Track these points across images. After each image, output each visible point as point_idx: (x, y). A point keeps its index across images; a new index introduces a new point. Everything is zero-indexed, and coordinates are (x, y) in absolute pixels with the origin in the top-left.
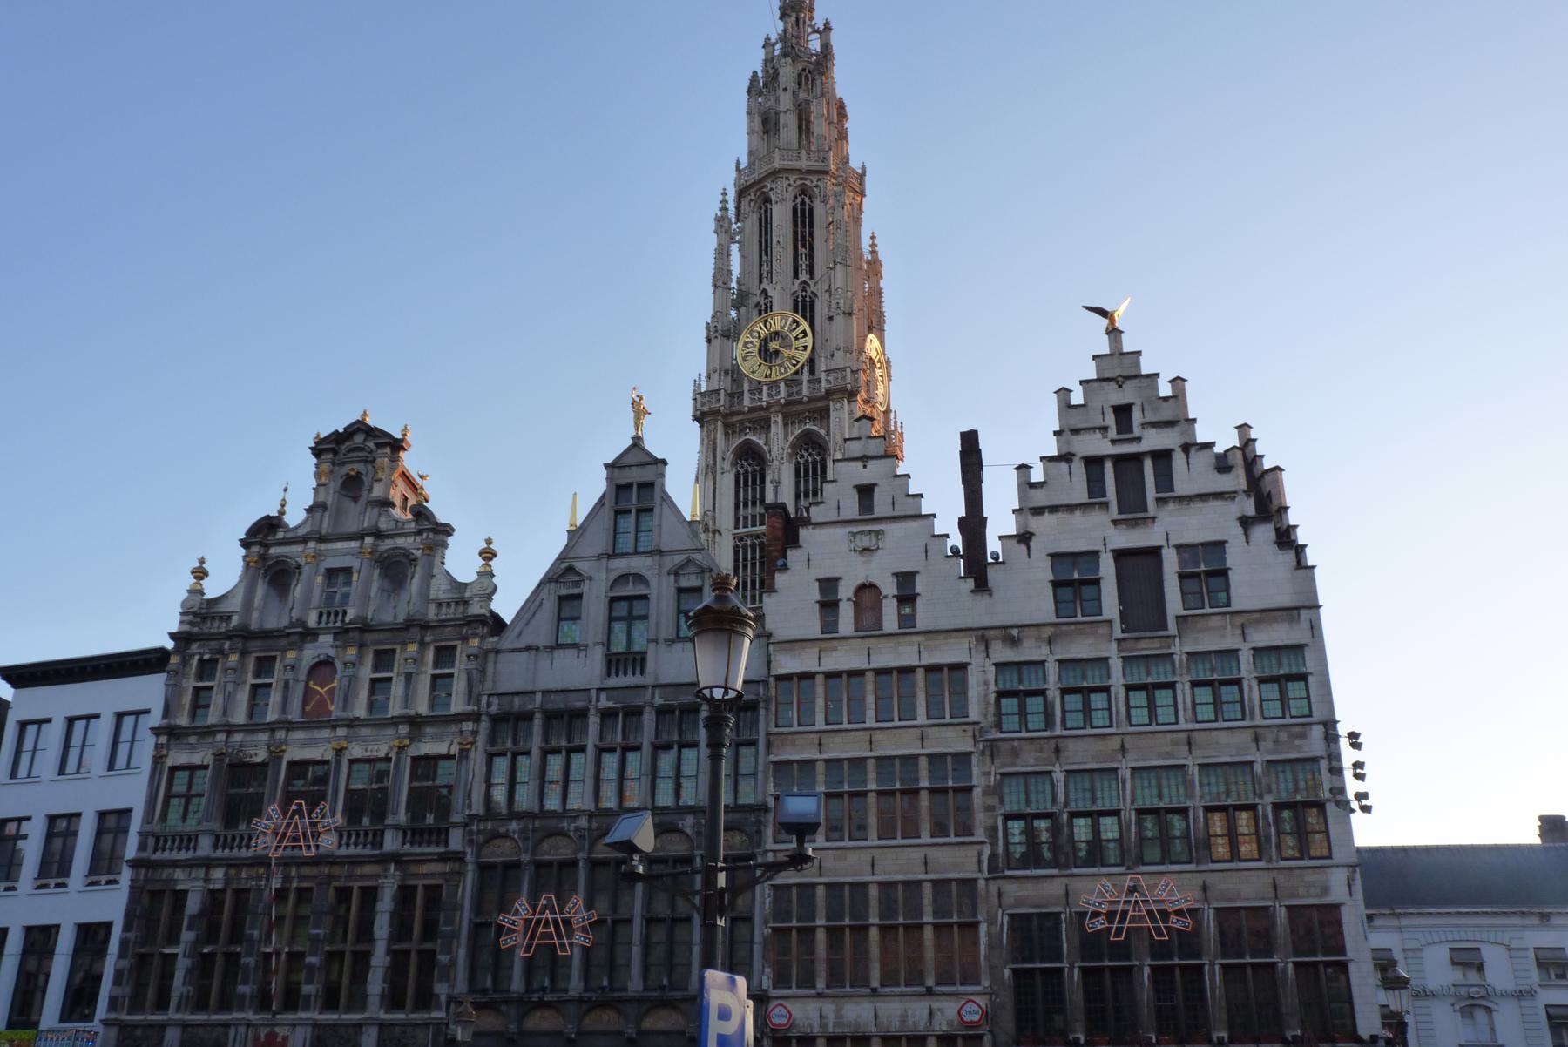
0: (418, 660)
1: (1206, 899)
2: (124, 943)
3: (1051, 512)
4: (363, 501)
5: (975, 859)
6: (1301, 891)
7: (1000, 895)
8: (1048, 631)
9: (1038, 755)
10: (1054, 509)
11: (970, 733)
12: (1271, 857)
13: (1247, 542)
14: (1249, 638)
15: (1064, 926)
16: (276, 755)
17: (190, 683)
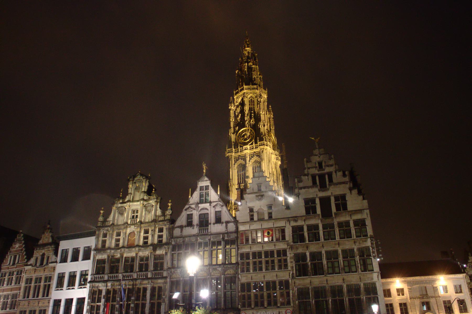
0: (154, 231)
1: (344, 282)
2: (88, 303)
3: (304, 189)
4: (140, 192)
5: (288, 275)
6: (366, 279)
7: (294, 283)
8: (304, 218)
9: (303, 249)
10: (304, 188)
11: (286, 244)
12: (359, 271)
13: (351, 194)
14: (352, 218)
15: (310, 290)
16: (122, 256)
17: (101, 239)
